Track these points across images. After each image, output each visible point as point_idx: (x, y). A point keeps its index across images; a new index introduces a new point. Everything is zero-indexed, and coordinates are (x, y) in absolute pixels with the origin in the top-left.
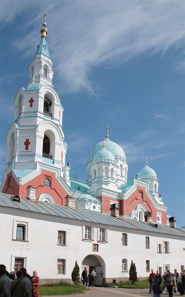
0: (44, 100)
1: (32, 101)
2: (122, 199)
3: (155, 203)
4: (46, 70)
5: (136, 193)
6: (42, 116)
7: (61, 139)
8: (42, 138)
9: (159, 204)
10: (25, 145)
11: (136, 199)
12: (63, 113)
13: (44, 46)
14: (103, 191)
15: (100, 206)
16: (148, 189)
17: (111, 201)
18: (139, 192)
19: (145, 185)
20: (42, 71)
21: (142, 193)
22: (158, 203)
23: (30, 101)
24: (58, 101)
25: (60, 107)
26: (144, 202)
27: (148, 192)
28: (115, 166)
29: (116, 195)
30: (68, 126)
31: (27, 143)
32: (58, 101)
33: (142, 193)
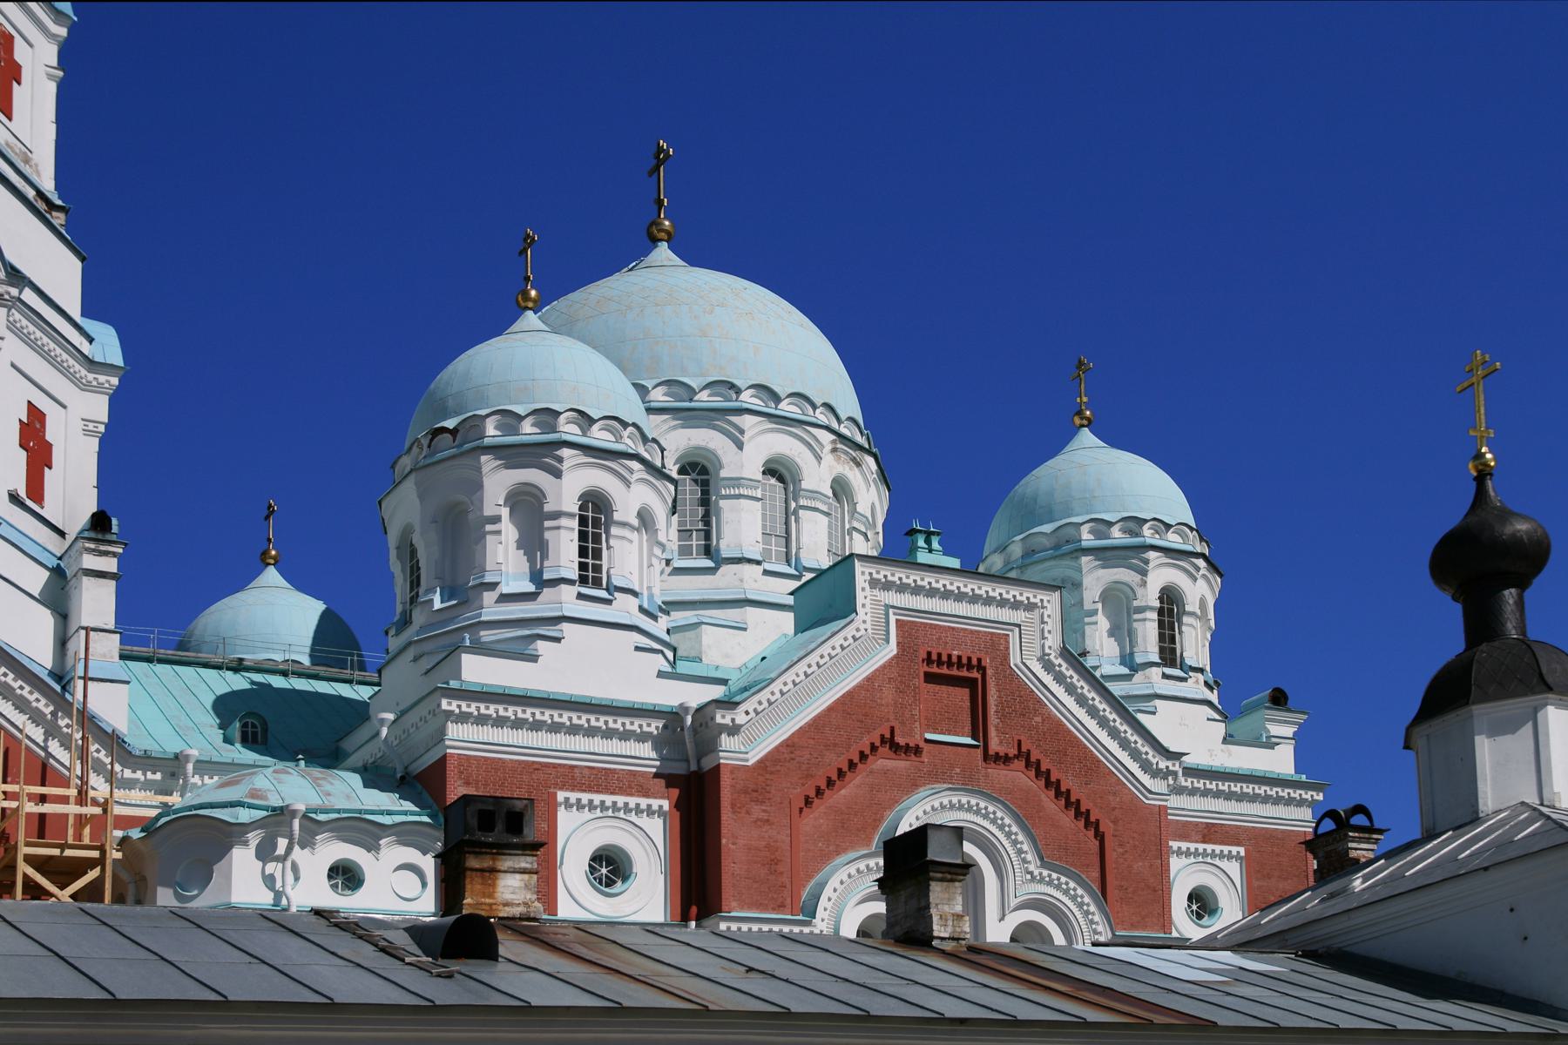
2: (707, 764)
3: (1146, 766)
5: (888, 694)
9: (1191, 772)
11: (885, 750)
14: (463, 718)
15: (428, 864)
16: (1053, 642)
17: (561, 796)
18: (930, 678)
19: (1016, 605)
21: (970, 683)
22: (1177, 756)
26: (999, 774)
27: (1048, 666)
28: (635, 465)
29: (642, 737)
33: (976, 689)
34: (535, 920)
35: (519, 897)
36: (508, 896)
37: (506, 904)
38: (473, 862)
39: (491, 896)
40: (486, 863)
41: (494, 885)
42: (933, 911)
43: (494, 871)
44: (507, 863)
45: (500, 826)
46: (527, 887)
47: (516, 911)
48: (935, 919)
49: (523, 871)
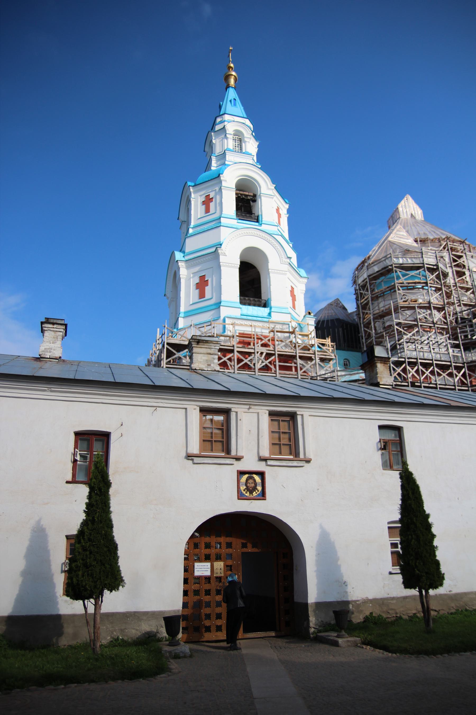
0: (236, 194)
1: (207, 201)
4: (240, 140)
6: (235, 222)
7: (284, 259)
10: (197, 289)
12: (289, 211)
13: (231, 101)
20: (230, 143)
23: (204, 203)
24: (270, 187)
25: (275, 198)
30: (302, 234)
31: (202, 284)
32: (269, 189)
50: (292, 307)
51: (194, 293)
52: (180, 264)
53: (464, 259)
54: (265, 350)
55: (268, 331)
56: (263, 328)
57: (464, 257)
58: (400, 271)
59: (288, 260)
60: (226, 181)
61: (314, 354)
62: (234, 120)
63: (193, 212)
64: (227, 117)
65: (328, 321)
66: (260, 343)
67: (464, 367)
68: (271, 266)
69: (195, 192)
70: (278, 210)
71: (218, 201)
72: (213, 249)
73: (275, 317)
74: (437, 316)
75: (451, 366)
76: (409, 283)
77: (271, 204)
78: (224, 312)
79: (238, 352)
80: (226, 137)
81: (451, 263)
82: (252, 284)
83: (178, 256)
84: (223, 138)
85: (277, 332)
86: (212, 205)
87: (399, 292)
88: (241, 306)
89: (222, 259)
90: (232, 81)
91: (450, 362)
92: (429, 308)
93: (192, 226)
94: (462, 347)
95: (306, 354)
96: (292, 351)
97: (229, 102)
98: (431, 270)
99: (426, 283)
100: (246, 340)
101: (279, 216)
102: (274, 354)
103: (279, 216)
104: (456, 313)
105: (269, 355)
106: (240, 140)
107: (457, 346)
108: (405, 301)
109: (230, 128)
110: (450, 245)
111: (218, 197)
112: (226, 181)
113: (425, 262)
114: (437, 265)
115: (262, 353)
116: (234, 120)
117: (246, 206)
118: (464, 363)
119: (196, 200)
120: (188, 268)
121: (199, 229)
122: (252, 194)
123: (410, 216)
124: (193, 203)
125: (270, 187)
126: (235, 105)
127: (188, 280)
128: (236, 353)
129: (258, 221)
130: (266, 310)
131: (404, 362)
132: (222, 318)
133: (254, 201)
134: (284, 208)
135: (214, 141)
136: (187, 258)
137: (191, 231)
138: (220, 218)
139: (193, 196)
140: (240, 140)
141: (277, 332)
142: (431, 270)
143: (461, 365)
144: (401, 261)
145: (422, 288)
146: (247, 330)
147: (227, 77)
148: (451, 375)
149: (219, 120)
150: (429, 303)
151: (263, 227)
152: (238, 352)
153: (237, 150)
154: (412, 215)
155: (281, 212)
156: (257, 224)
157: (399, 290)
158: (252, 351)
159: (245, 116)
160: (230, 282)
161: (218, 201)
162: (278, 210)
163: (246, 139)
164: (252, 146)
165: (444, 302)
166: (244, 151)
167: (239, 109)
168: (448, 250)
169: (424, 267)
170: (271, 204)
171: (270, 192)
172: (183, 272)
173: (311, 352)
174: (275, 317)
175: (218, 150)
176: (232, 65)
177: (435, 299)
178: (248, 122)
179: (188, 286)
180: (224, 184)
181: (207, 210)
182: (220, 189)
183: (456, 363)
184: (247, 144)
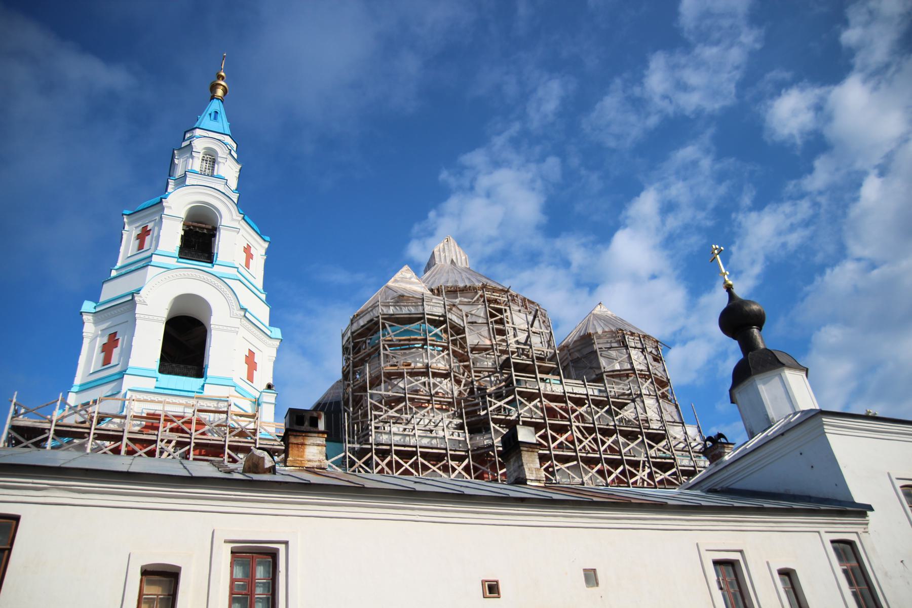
1: (144, 233)
6: (173, 262)
8: (158, 321)
20: (197, 164)
24: (235, 217)
25: (242, 231)
32: (233, 220)
34: (324, 469)
35: (317, 458)
36: (311, 457)
37: (309, 461)
38: (292, 440)
39: (302, 457)
40: (300, 440)
41: (303, 452)
42: (525, 467)
43: (303, 444)
44: (309, 441)
45: (306, 423)
46: (320, 453)
47: (315, 464)
48: (526, 470)
49: (318, 445)
50: (245, 377)
51: (98, 357)
52: (85, 317)
53: (508, 313)
54: (175, 437)
55: (191, 411)
56: (187, 406)
57: (508, 311)
58: (390, 326)
59: (242, 313)
60: (170, 208)
61: (255, 443)
62: (211, 138)
63: (122, 249)
64: (198, 132)
65: (331, 403)
66: (169, 425)
67: (468, 456)
68: (213, 320)
69: (130, 223)
70: (247, 250)
71: (155, 234)
72: (130, 298)
73: (209, 391)
74: (446, 385)
75: (446, 455)
76: (400, 340)
77: (237, 239)
78: (128, 382)
79: (129, 439)
80: (192, 157)
81: (487, 319)
82: (185, 345)
83: (88, 306)
84: (188, 158)
85: (199, 411)
86: (148, 239)
87: (386, 352)
88: (160, 376)
89: (139, 309)
90: (220, 92)
91: (446, 449)
92: (425, 374)
93: (116, 267)
94: (466, 428)
95: (242, 442)
96: (220, 438)
97: (207, 115)
98: (436, 323)
99: (425, 340)
100: (152, 421)
101: (249, 256)
102: (189, 443)
103: (249, 256)
104: (472, 382)
105: (180, 445)
106: (211, 159)
107: (460, 427)
108: (395, 366)
109: (199, 145)
110: (488, 295)
111: (156, 229)
112: (170, 208)
113: (426, 311)
114: (444, 316)
115: (169, 442)
116: (211, 138)
117: (199, 241)
118: (467, 451)
119: (130, 234)
120: (96, 323)
121: (123, 271)
122: (210, 227)
123: (449, 262)
124: (125, 237)
125: (235, 217)
126: (215, 118)
127: (94, 340)
128: (125, 440)
129: (211, 262)
130: (200, 381)
131: (370, 450)
132: (123, 392)
133: (214, 236)
134: (260, 248)
135: (176, 161)
136: (98, 310)
137: (114, 273)
138: (151, 256)
139: (127, 227)
140: (214, 161)
141: (199, 411)
142: (436, 323)
143: (463, 453)
144: (391, 310)
145: (422, 347)
146: (156, 408)
147: (214, 87)
148: (445, 469)
149: (188, 135)
150: (427, 367)
151: (216, 269)
152: (129, 439)
153: (209, 173)
154: (452, 261)
155: (253, 251)
156: (210, 265)
157: (385, 349)
158: (154, 438)
159: (228, 131)
160: (148, 341)
161: (155, 234)
162: (247, 250)
163: (219, 160)
164: (229, 170)
165: (450, 366)
166: (215, 174)
167: (223, 124)
168: (484, 301)
169: (423, 318)
170: (237, 239)
171: (236, 225)
172: (89, 328)
173: (249, 440)
174: (209, 391)
175: (179, 172)
176: (223, 74)
177: (439, 363)
178: (228, 140)
179: (92, 349)
180: (166, 211)
181: (141, 247)
182: (161, 217)
183: (455, 451)
184: (221, 165)
